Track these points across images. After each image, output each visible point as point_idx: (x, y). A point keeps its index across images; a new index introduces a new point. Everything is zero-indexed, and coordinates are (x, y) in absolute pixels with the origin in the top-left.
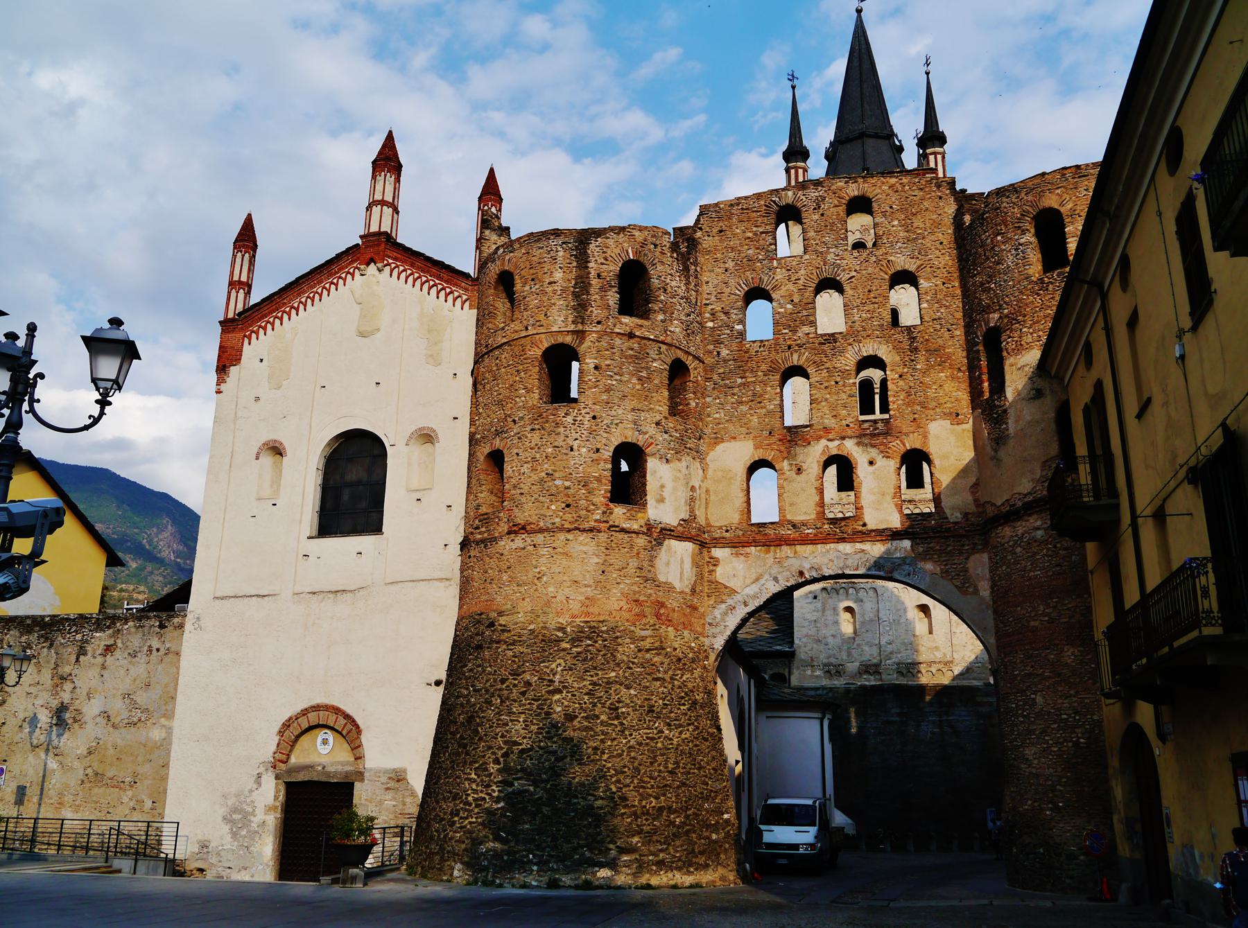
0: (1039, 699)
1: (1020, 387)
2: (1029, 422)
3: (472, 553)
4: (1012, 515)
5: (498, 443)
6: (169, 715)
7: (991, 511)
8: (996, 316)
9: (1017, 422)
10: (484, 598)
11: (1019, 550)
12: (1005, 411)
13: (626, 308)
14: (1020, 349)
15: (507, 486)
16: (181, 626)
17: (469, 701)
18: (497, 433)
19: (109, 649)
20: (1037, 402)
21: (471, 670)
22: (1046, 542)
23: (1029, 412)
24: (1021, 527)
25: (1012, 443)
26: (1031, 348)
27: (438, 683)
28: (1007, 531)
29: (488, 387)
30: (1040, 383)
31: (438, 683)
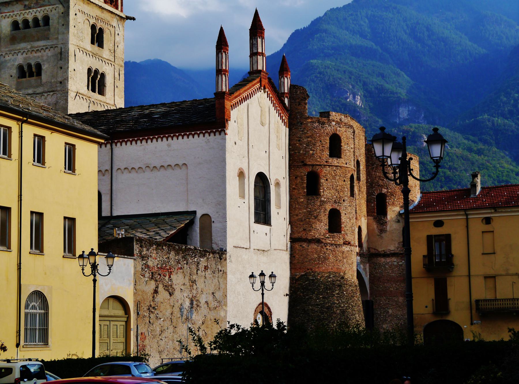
0: (390, 311)
1: (393, 217)
2: (395, 229)
3: (328, 247)
4: (385, 255)
5: (336, 206)
6: (226, 305)
7: (373, 251)
8: (386, 190)
9: (390, 227)
10: (335, 267)
11: (387, 266)
12: (386, 222)
13: (332, 155)
14: (393, 204)
15: (343, 226)
16: (226, 260)
17: (340, 306)
18: (335, 202)
19: (206, 268)
20: (398, 224)
21: (337, 294)
22: (396, 266)
23: (395, 226)
24: (388, 260)
25: (388, 233)
26: (396, 206)
27: (287, 295)
28: (383, 260)
29: (329, 180)
30: (399, 218)
31: (287, 295)
